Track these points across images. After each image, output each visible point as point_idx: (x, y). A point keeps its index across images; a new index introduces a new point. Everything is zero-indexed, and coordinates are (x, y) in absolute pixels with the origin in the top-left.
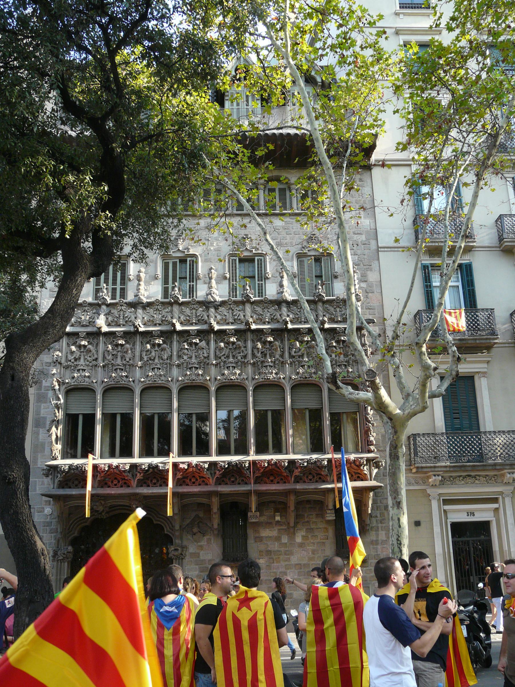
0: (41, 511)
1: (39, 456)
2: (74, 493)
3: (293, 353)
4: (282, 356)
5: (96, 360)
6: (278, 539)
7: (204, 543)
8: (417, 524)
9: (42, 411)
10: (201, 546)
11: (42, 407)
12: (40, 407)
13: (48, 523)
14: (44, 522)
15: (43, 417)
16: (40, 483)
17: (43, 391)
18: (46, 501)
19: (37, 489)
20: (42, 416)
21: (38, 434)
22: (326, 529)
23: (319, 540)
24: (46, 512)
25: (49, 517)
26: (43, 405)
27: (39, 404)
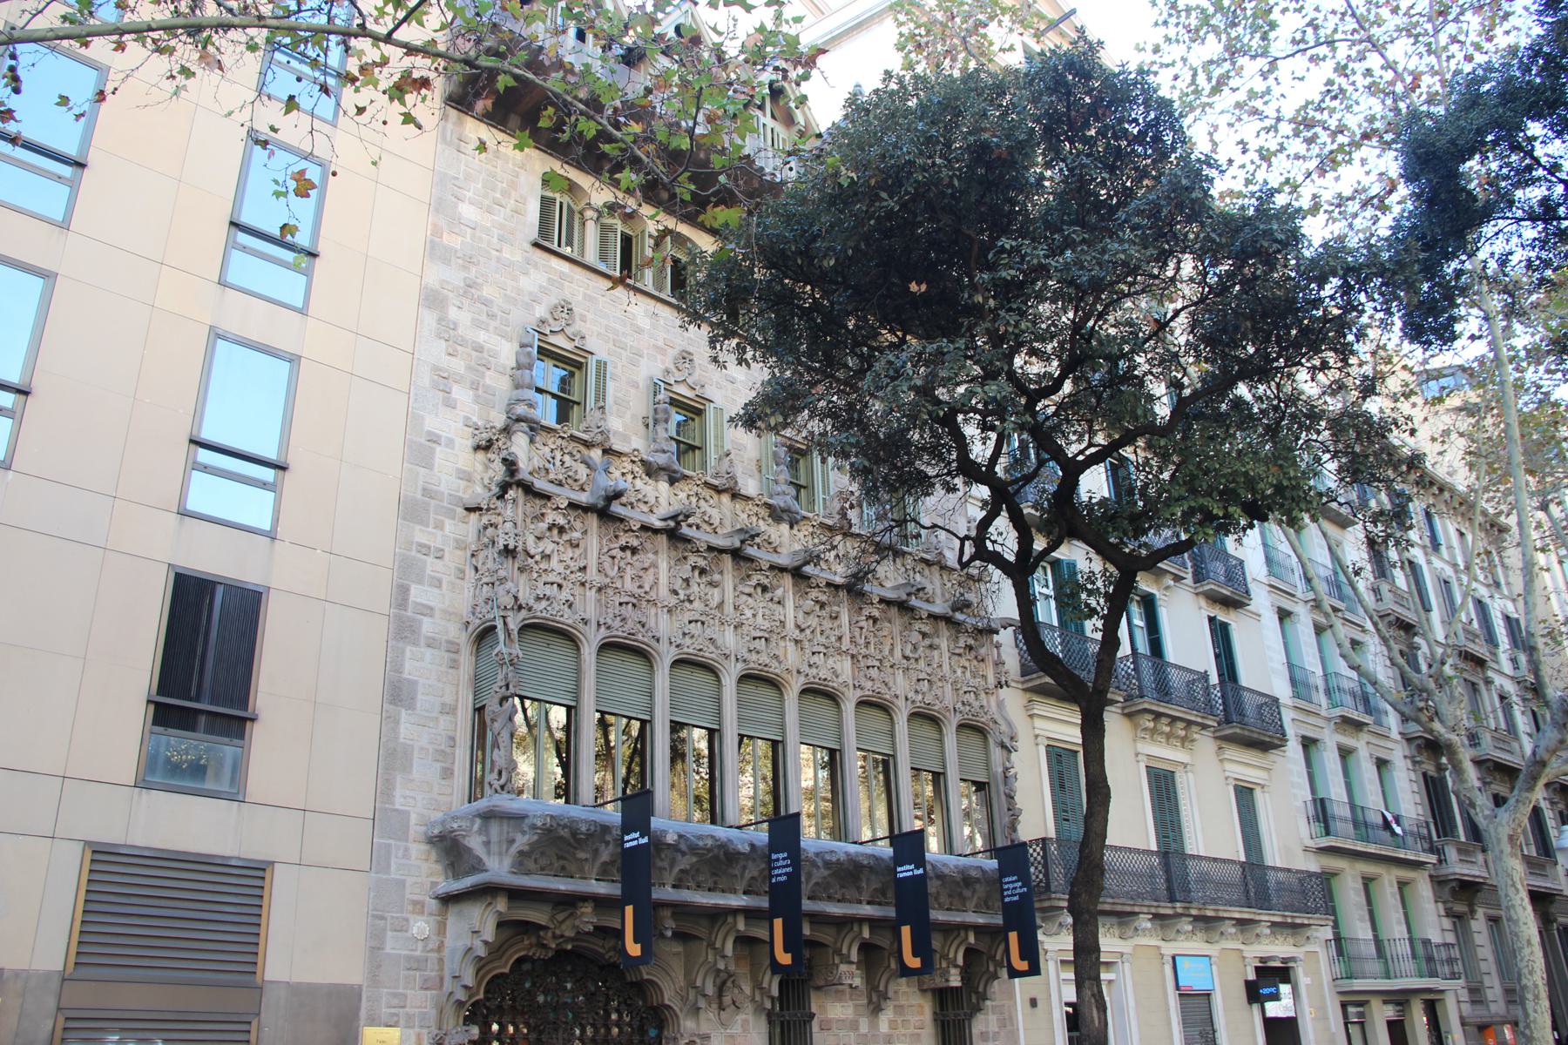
0: (402, 927)
1: (399, 779)
2: (562, 887)
3: (908, 653)
4: (891, 651)
5: (583, 569)
6: (854, 1026)
7: (736, 1029)
8: (1033, 1003)
9: (409, 666)
10: (732, 1036)
11: (408, 654)
12: (403, 652)
13: (417, 960)
14: (408, 958)
15: (409, 681)
16: (400, 854)
17: (409, 613)
18: (415, 903)
19: (393, 867)
20: (406, 676)
21: (397, 722)
22: (921, 1006)
23: (912, 1030)
24: (415, 931)
25: (420, 945)
26: (409, 649)
27: (401, 645)
